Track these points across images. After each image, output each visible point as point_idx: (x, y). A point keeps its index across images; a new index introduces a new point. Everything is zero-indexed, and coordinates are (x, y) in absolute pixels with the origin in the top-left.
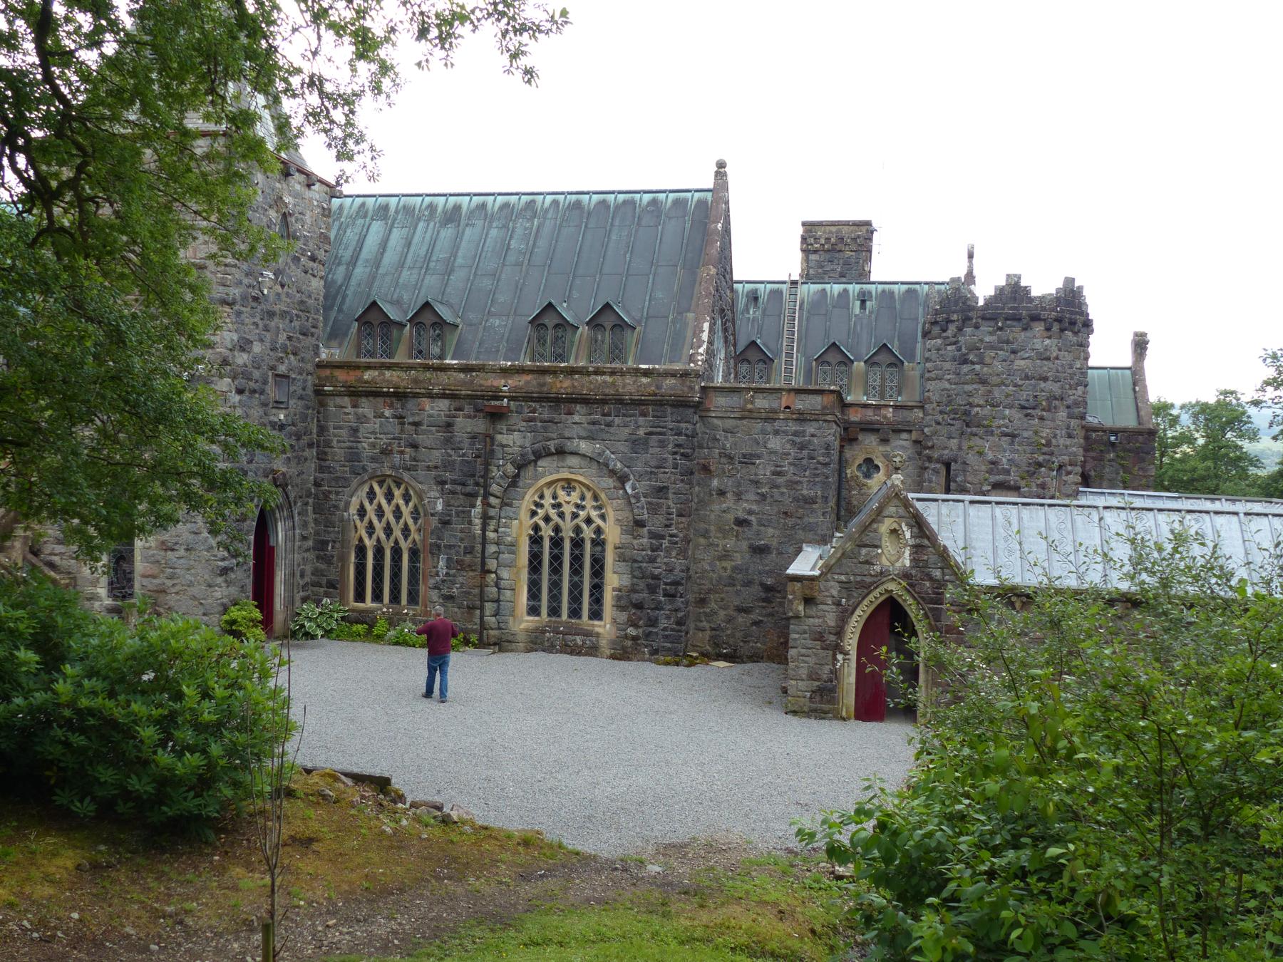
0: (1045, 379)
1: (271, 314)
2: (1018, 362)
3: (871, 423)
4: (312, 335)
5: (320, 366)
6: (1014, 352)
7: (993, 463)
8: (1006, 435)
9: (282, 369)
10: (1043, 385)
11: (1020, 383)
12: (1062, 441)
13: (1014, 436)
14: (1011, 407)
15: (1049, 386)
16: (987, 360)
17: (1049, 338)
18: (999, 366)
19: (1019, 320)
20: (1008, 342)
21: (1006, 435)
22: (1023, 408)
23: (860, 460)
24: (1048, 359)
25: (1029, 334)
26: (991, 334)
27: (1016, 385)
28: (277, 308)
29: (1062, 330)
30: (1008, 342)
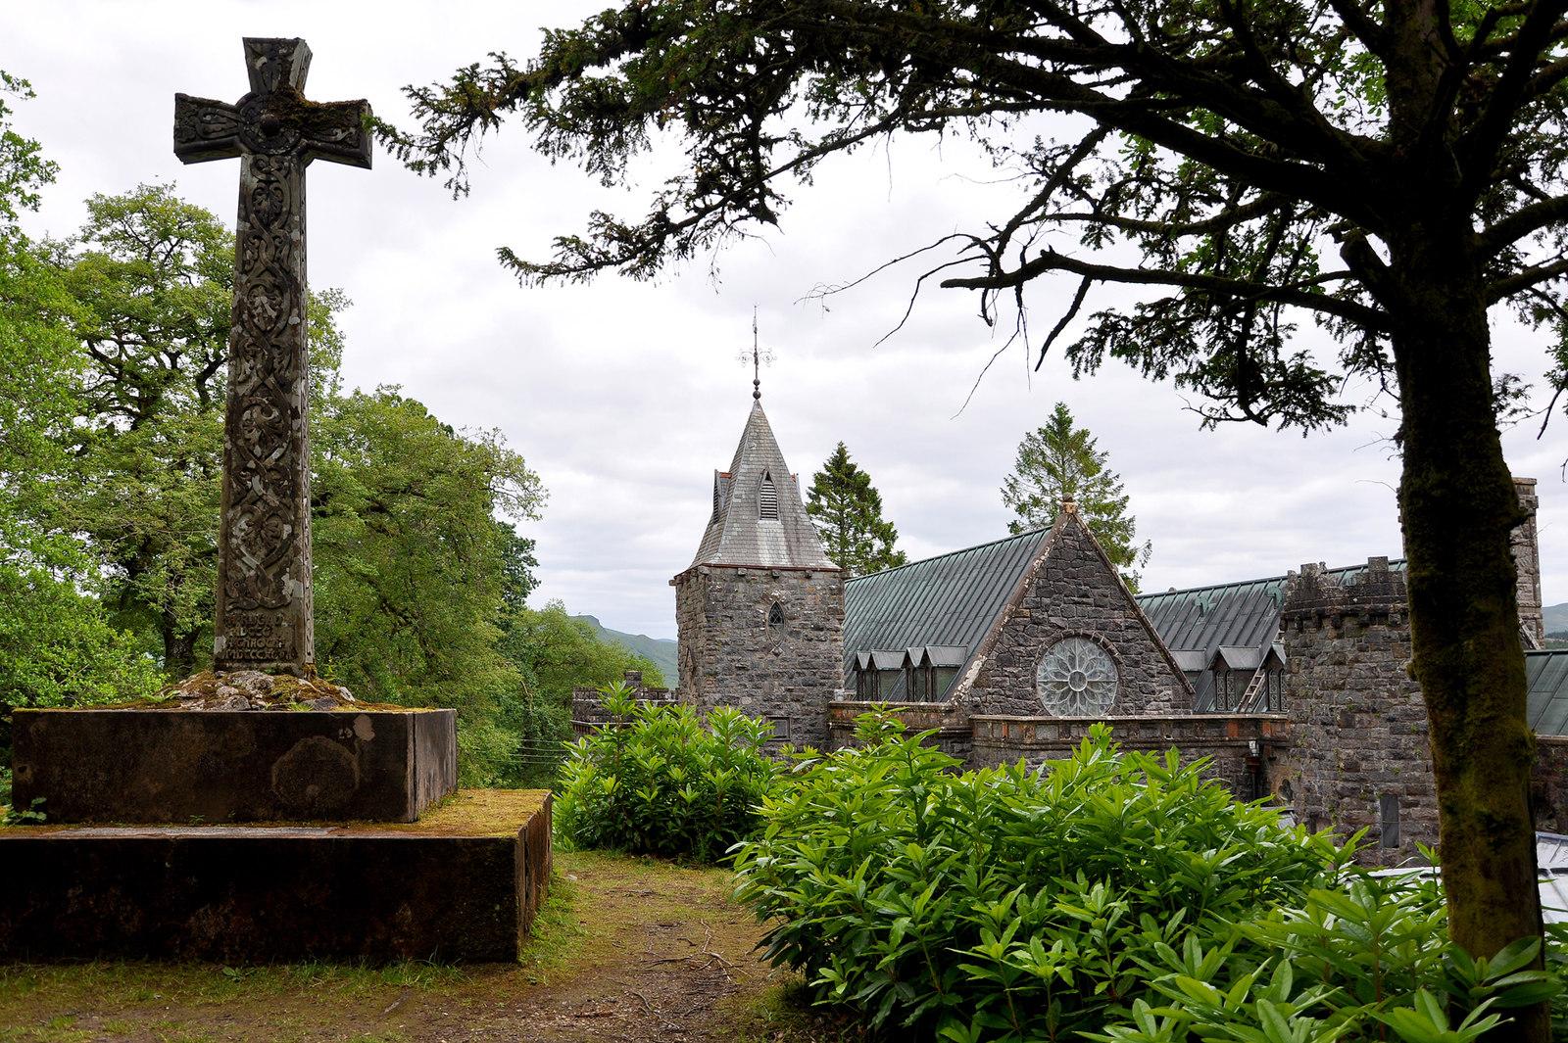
0: (1340, 688)
1: (763, 677)
2: (1317, 669)
3: (1279, 740)
4: (823, 685)
5: (831, 706)
6: (1313, 657)
7: (1308, 790)
8: (1314, 756)
9: (778, 713)
10: (1336, 694)
11: (1319, 693)
12: (1382, 766)
13: (1321, 758)
14: (1315, 723)
15: (1347, 696)
16: (1295, 668)
17: (1339, 637)
18: (1303, 676)
19: (1310, 619)
20: (1305, 645)
21: (1314, 756)
22: (1324, 724)
23: (1279, 784)
24: (1341, 663)
25: (1320, 635)
26: (1296, 637)
27: (1317, 697)
28: (771, 670)
29: (1364, 626)
30: (1305, 645)
